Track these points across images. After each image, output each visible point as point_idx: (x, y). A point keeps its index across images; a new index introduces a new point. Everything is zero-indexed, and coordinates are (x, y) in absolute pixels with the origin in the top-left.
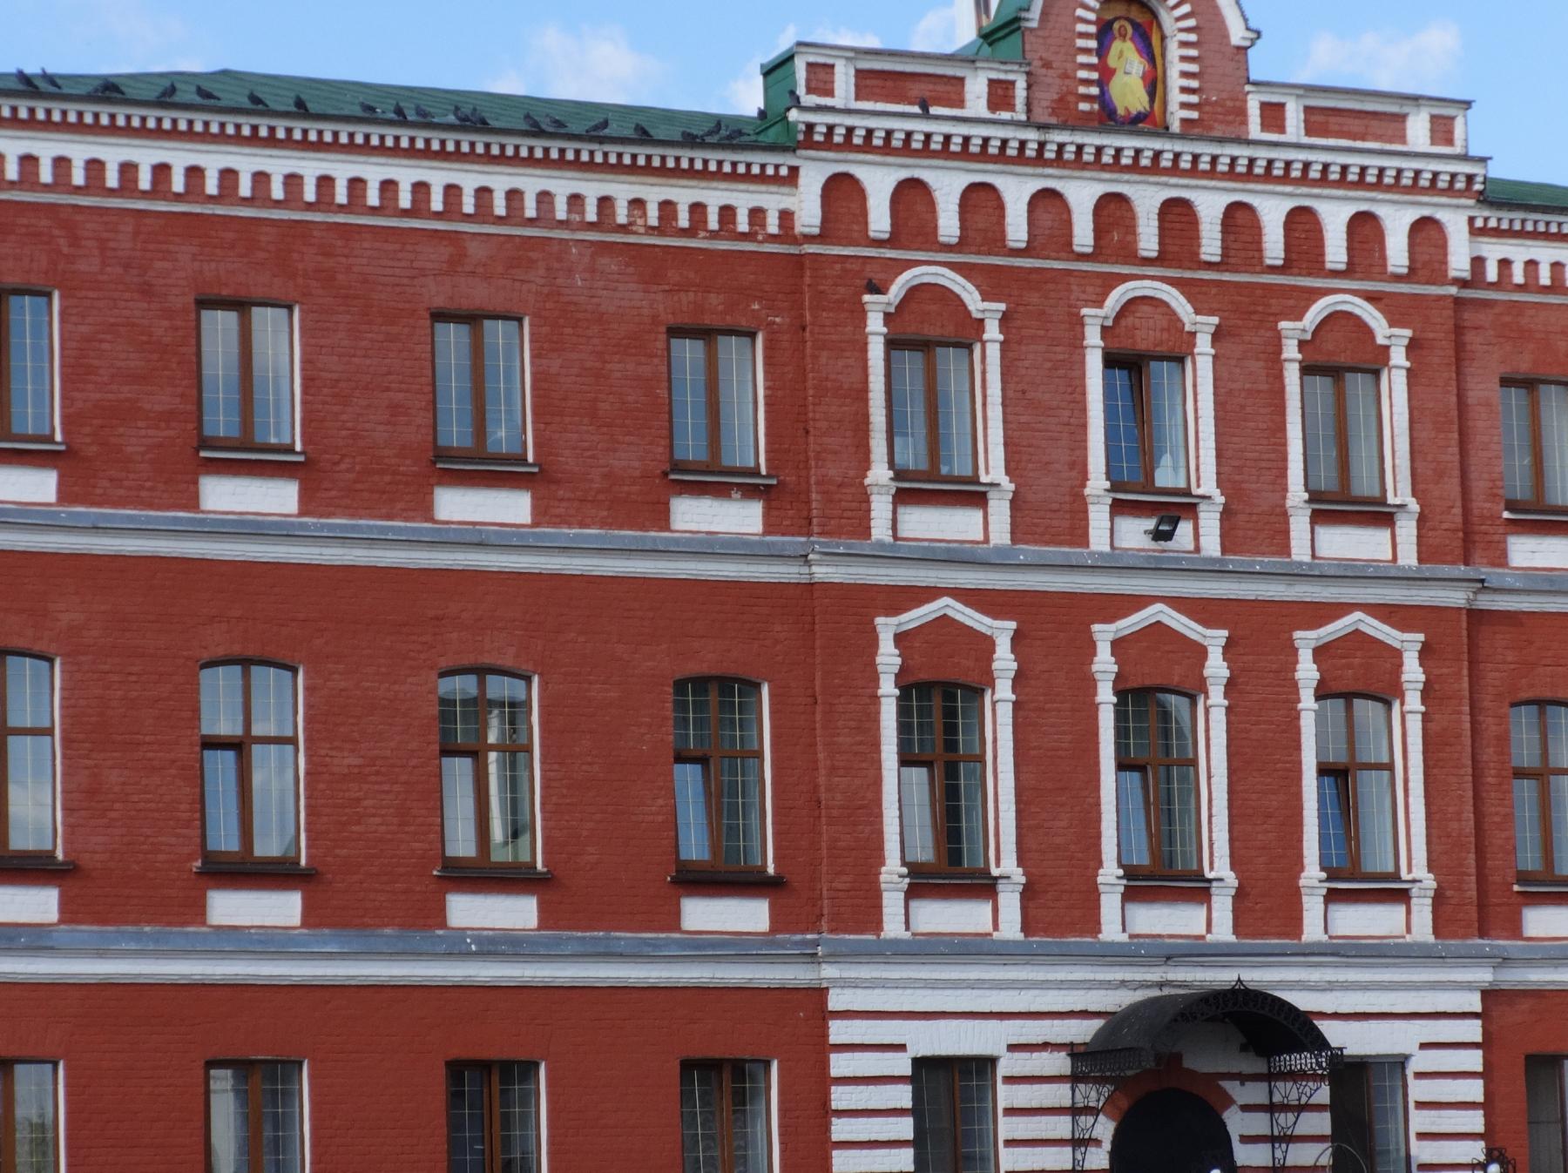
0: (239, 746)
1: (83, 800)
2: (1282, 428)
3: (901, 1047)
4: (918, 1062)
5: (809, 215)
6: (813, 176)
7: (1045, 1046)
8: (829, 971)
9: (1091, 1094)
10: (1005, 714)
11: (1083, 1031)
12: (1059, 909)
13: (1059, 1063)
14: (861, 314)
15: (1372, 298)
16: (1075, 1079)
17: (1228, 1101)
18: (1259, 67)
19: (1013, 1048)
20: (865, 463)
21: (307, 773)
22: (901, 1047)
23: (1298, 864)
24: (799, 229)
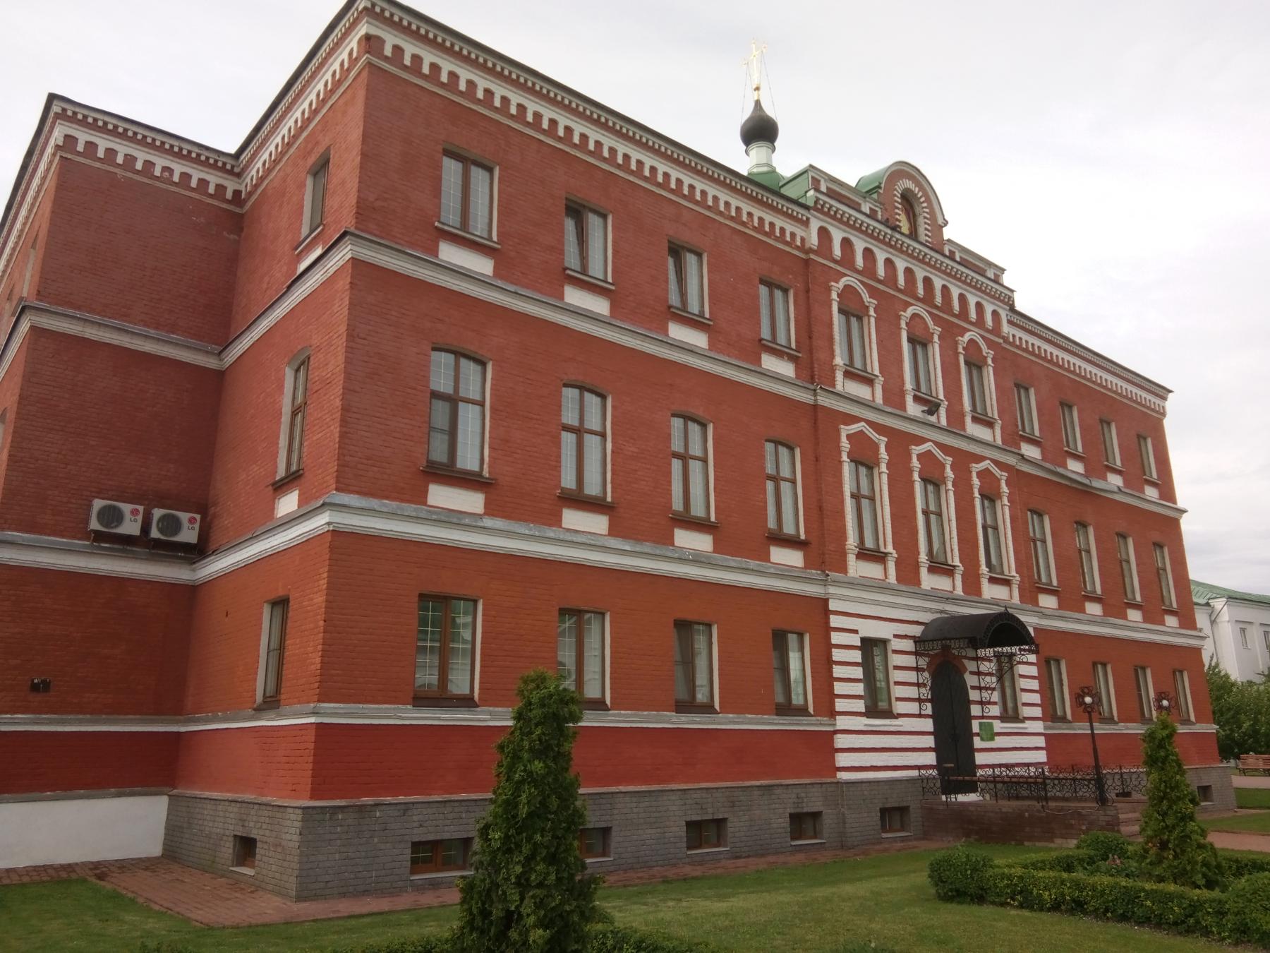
0: (579, 431)
1: (501, 445)
2: (959, 380)
3: (856, 632)
4: (863, 640)
5: (814, 240)
6: (815, 225)
7: (906, 637)
8: (832, 590)
9: (923, 662)
10: (885, 478)
11: (917, 631)
12: (908, 573)
13: (909, 645)
14: (829, 290)
15: (983, 337)
16: (916, 653)
17: (966, 669)
18: (948, 233)
19: (895, 636)
20: (833, 356)
21: (613, 452)
22: (856, 632)
23: (978, 565)
24: (807, 246)
